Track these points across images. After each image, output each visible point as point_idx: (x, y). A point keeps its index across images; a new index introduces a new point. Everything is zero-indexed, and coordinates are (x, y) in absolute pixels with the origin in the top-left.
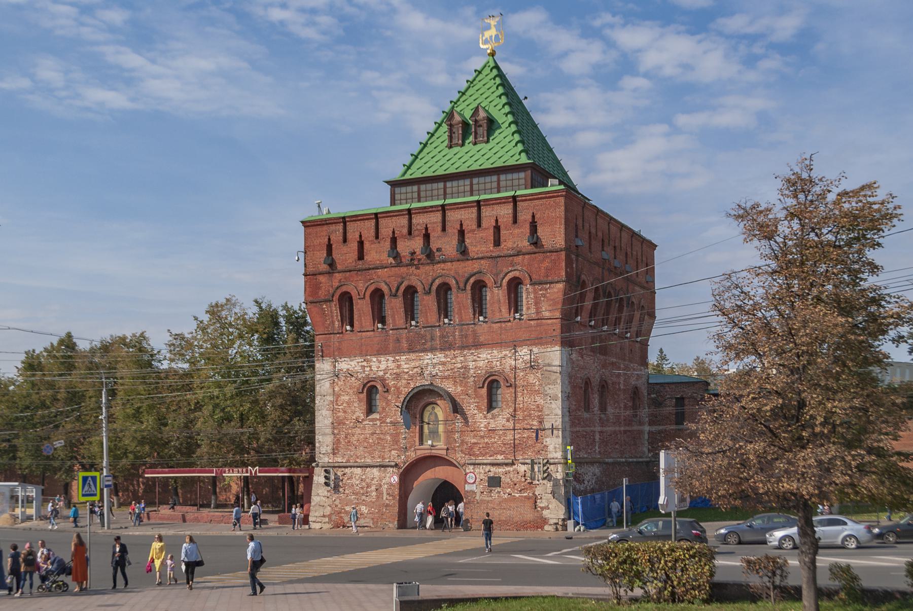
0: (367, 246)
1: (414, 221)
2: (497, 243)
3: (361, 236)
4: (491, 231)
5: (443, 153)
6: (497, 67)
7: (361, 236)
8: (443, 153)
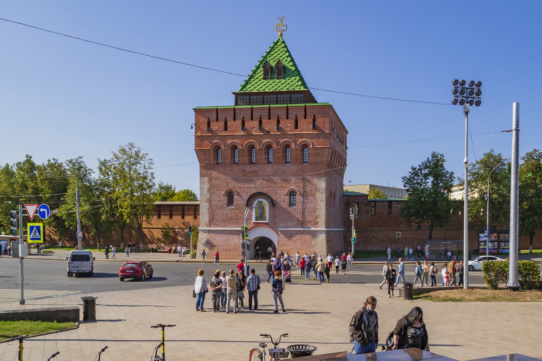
0: (229, 123)
1: (254, 114)
2: (296, 127)
3: (226, 119)
4: (294, 121)
5: (261, 81)
6: (284, 42)
7: (226, 119)
8: (261, 81)
